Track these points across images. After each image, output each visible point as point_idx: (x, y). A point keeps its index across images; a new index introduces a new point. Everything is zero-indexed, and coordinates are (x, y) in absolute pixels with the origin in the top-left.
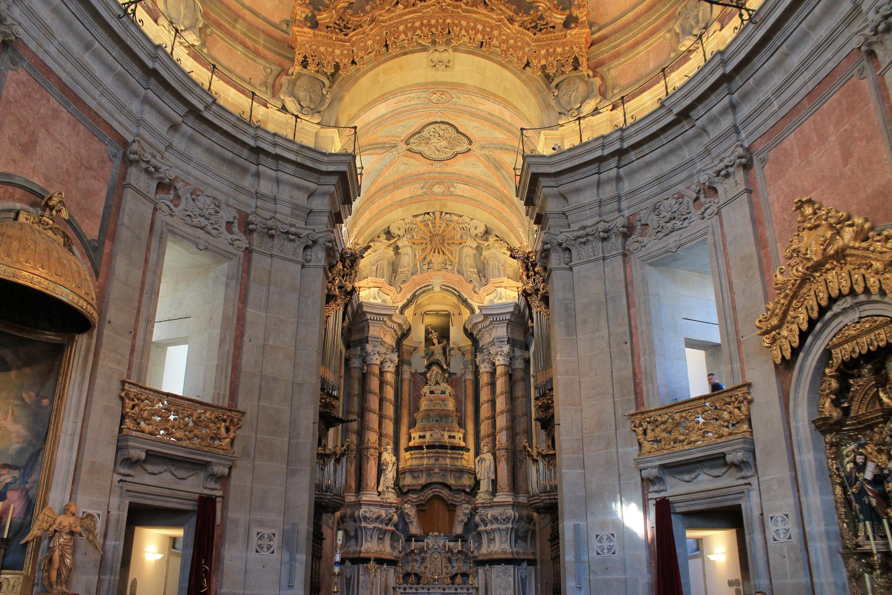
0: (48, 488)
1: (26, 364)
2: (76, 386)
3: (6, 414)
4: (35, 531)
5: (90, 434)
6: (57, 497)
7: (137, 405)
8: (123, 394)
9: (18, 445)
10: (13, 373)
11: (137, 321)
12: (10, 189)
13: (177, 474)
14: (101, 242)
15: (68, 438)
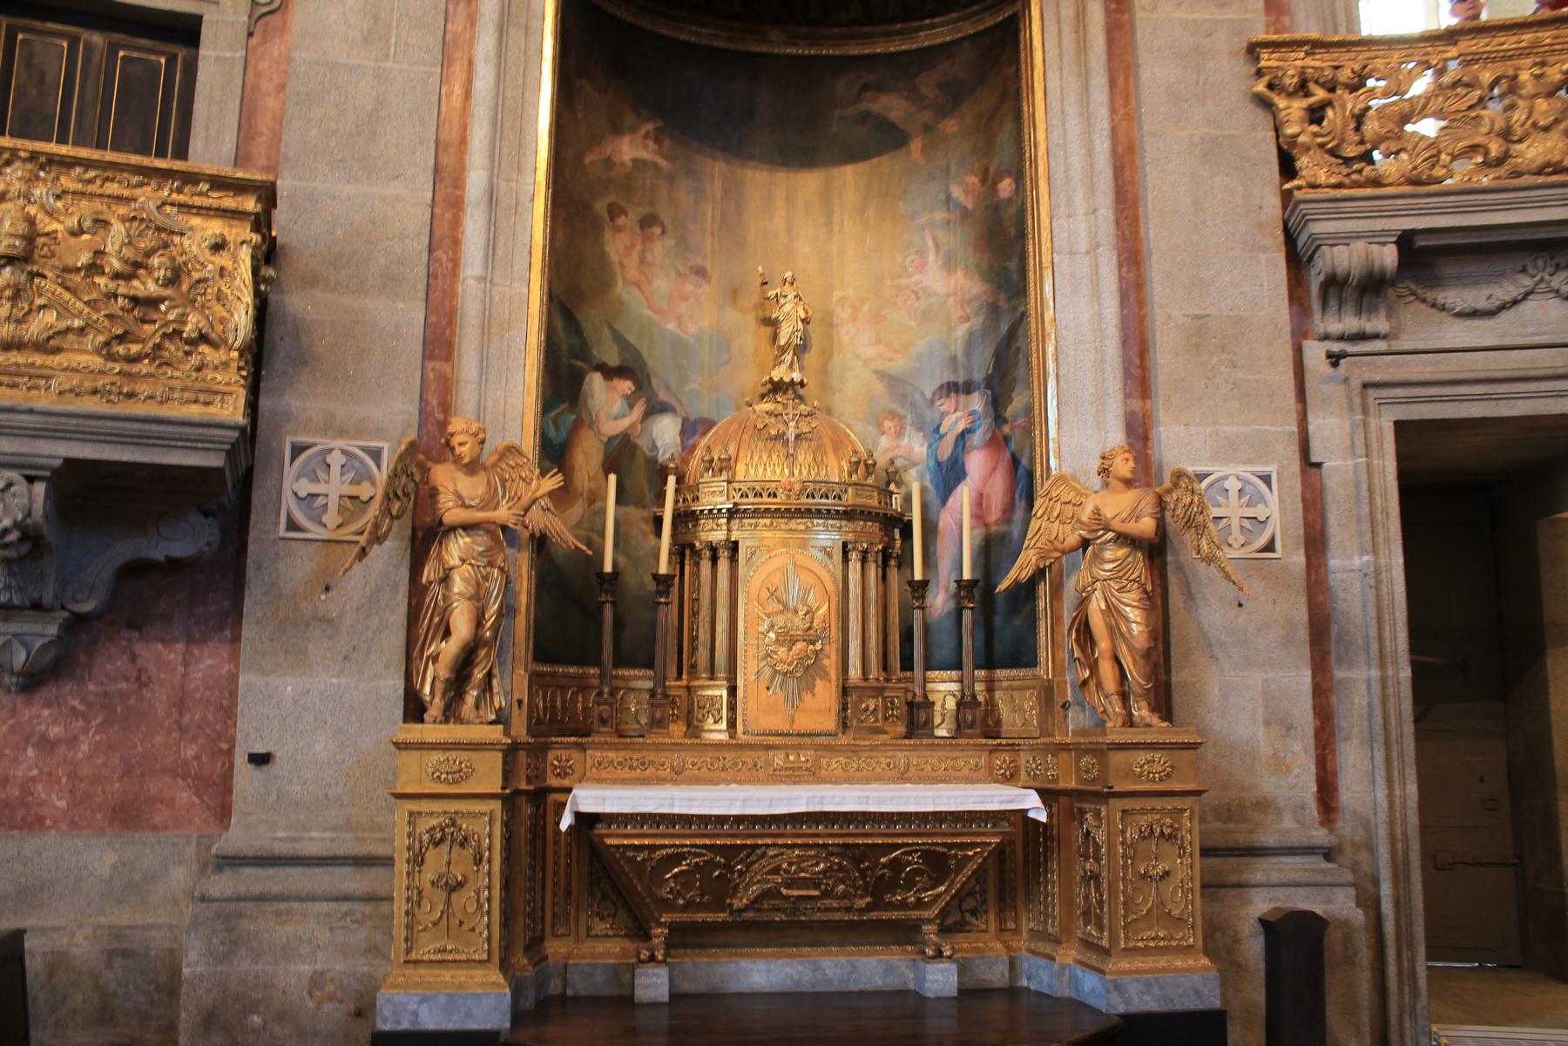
1: (943, 112)
5: (1158, 236)
7: (1329, 103)
8: (1260, 87)
9: (967, 325)
10: (915, 146)
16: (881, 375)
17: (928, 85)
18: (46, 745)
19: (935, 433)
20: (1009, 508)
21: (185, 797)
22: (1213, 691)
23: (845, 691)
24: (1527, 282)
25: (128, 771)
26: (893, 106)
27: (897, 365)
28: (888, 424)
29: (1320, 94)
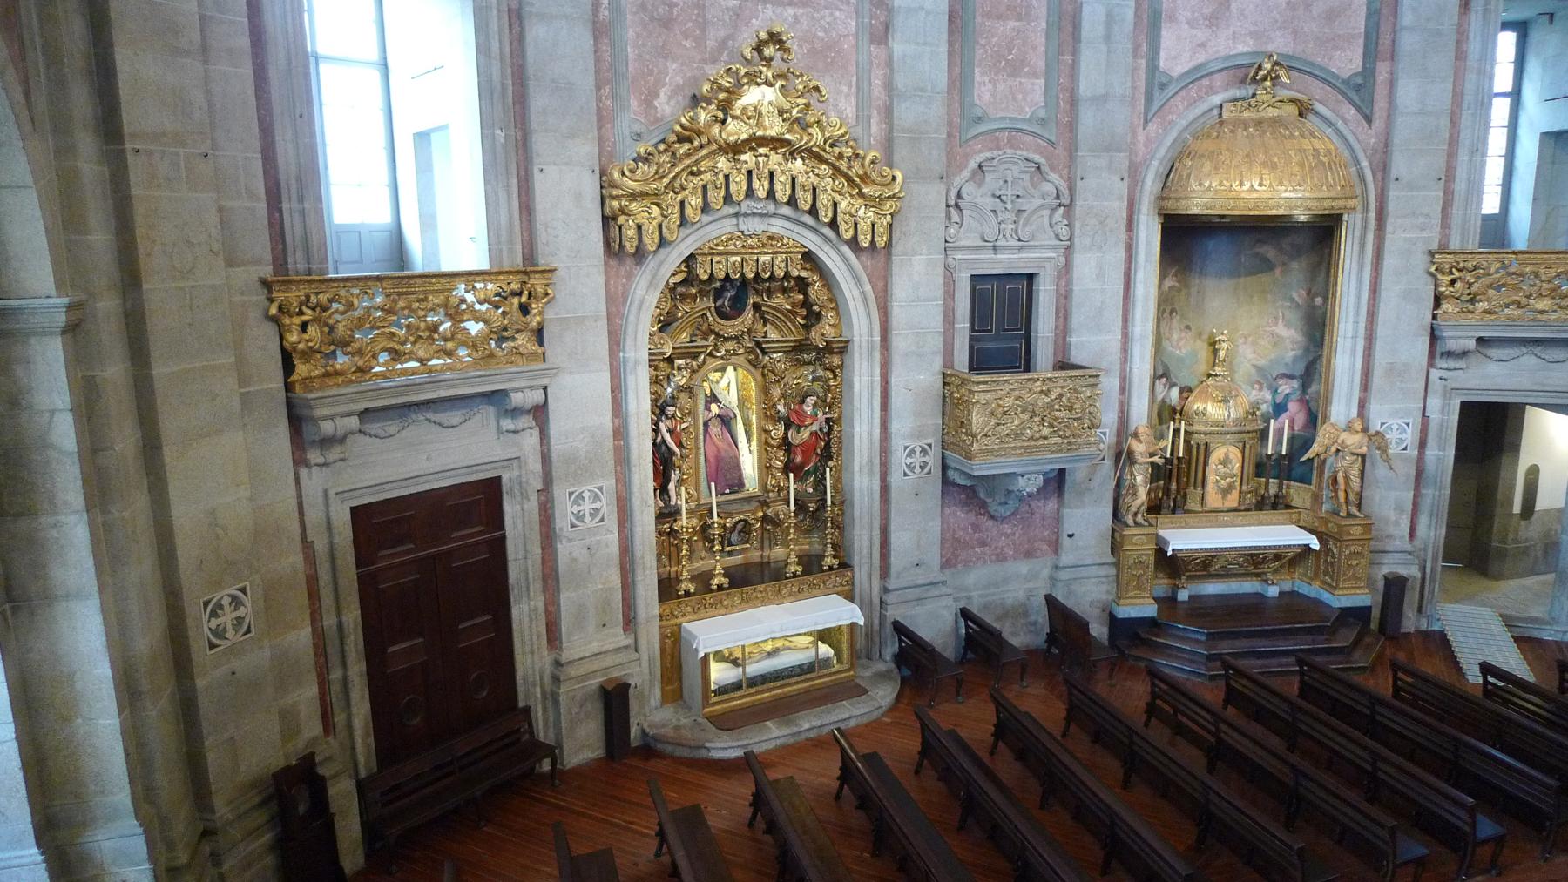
0: (1328, 401)
1: (1292, 258)
2: (1354, 277)
3: (1276, 318)
4: (1316, 448)
5: (1382, 331)
6: (1341, 409)
9: (1294, 352)
10: (1278, 271)
11: (1452, 155)
12: (1205, 82)
13: (1547, 357)
14: (1368, 72)
15: (1349, 342)
16: (1254, 366)
17: (1286, 243)
18: (1007, 536)
19: (1275, 392)
20: (1305, 426)
21: (1045, 547)
22: (1377, 498)
23: (1240, 492)
24: (1524, 350)
25: (1029, 541)
26: (1269, 251)
27: (1262, 362)
28: (1256, 386)
29: (1457, 274)
